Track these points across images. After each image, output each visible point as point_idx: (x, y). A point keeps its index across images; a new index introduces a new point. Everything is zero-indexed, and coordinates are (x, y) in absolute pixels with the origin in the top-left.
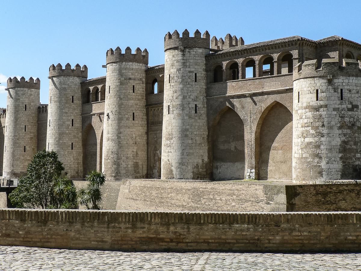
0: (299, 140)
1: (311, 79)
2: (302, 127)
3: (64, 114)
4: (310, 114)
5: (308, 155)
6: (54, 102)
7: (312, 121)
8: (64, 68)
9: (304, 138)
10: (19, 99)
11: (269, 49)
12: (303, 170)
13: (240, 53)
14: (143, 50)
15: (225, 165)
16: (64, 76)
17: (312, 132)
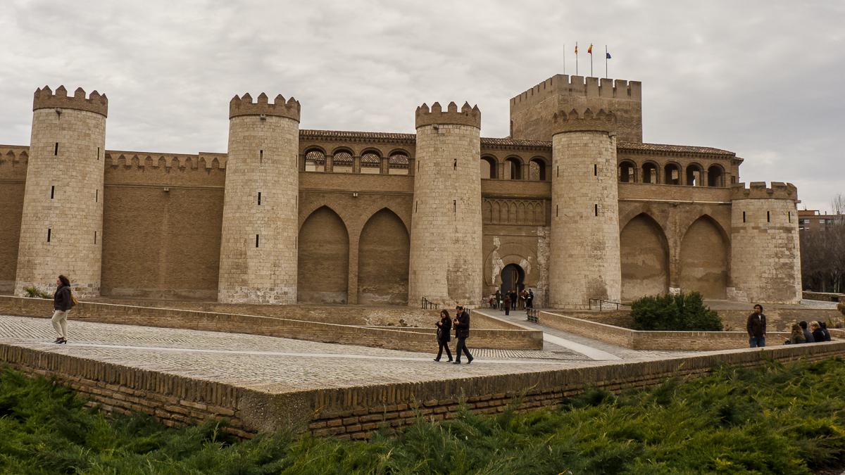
0: (771, 260)
1: (783, 201)
2: (776, 247)
3: (289, 186)
4: (784, 235)
5: (784, 276)
6: (270, 161)
7: (786, 242)
8: (255, 101)
9: (779, 258)
10: (89, 135)
11: (700, 157)
12: (779, 290)
13: (663, 154)
14: (430, 105)
15: (629, 283)
16: (289, 118)
17: (787, 253)
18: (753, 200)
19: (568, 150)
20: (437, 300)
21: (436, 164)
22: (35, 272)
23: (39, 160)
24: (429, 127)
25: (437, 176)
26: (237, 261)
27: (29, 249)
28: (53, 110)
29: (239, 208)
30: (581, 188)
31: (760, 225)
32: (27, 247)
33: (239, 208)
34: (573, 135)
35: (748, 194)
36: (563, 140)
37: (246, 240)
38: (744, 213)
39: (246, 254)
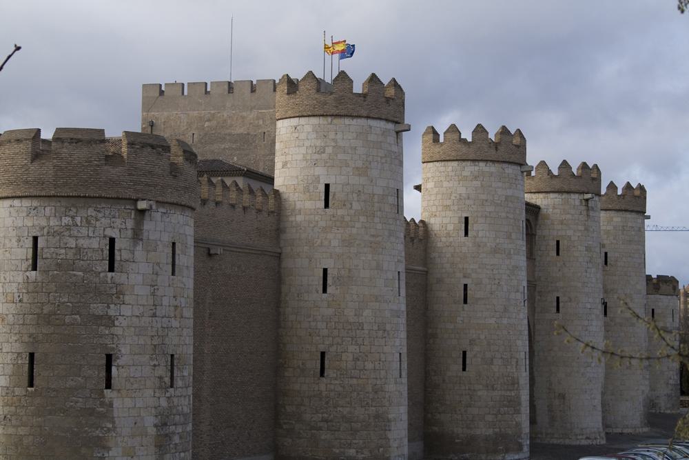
18: (662, 297)
19: (623, 234)
20: (595, 433)
21: (588, 249)
22: (390, 435)
23: (377, 220)
24: (577, 196)
25: (590, 265)
26: (508, 393)
27: (376, 392)
28: (390, 126)
29: (506, 310)
30: (637, 283)
31: (668, 325)
32: (370, 389)
33: (506, 310)
34: (628, 215)
35: (659, 289)
36: (615, 219)
37: (517, 362)
38: (653, 310)
39: (518, 383)
